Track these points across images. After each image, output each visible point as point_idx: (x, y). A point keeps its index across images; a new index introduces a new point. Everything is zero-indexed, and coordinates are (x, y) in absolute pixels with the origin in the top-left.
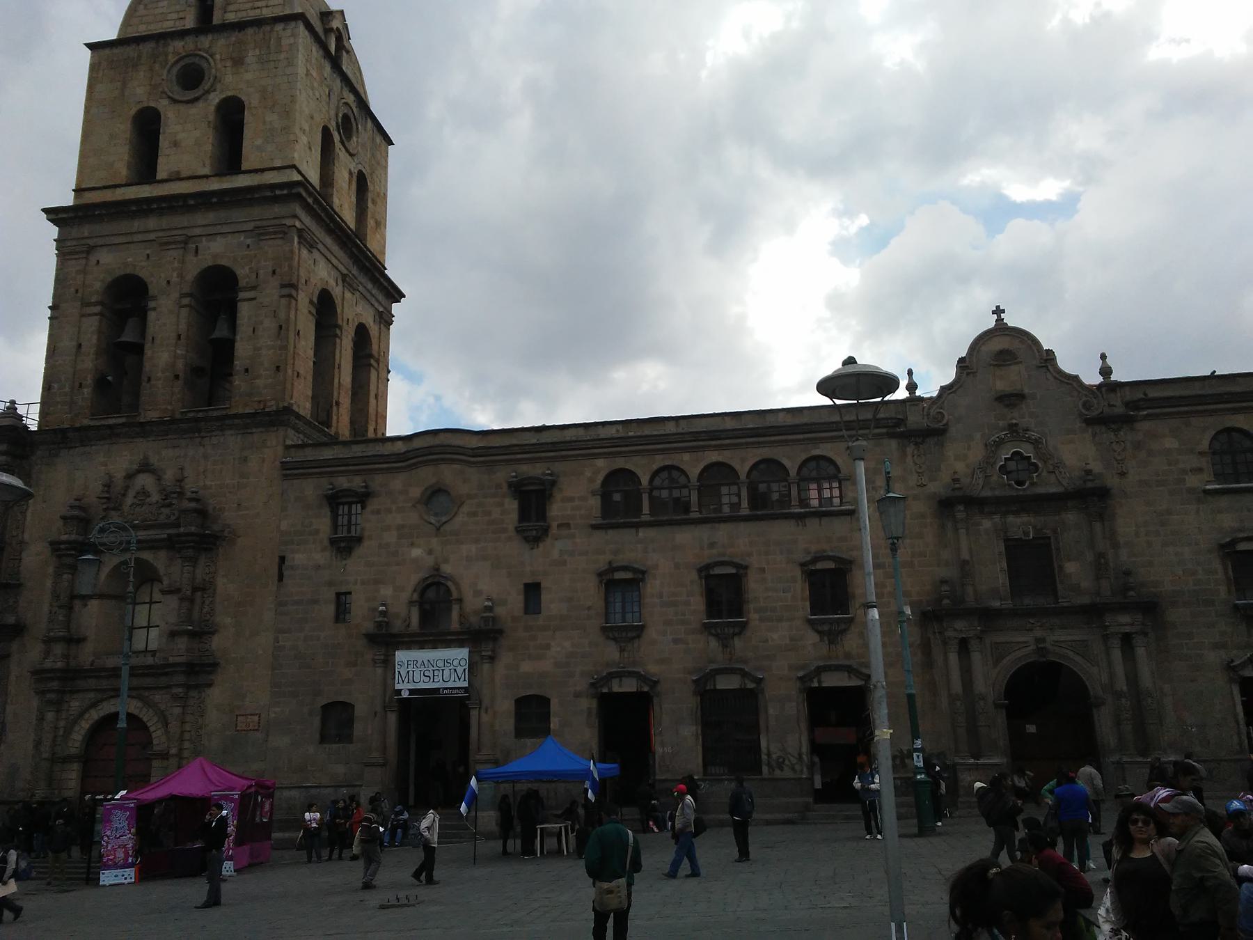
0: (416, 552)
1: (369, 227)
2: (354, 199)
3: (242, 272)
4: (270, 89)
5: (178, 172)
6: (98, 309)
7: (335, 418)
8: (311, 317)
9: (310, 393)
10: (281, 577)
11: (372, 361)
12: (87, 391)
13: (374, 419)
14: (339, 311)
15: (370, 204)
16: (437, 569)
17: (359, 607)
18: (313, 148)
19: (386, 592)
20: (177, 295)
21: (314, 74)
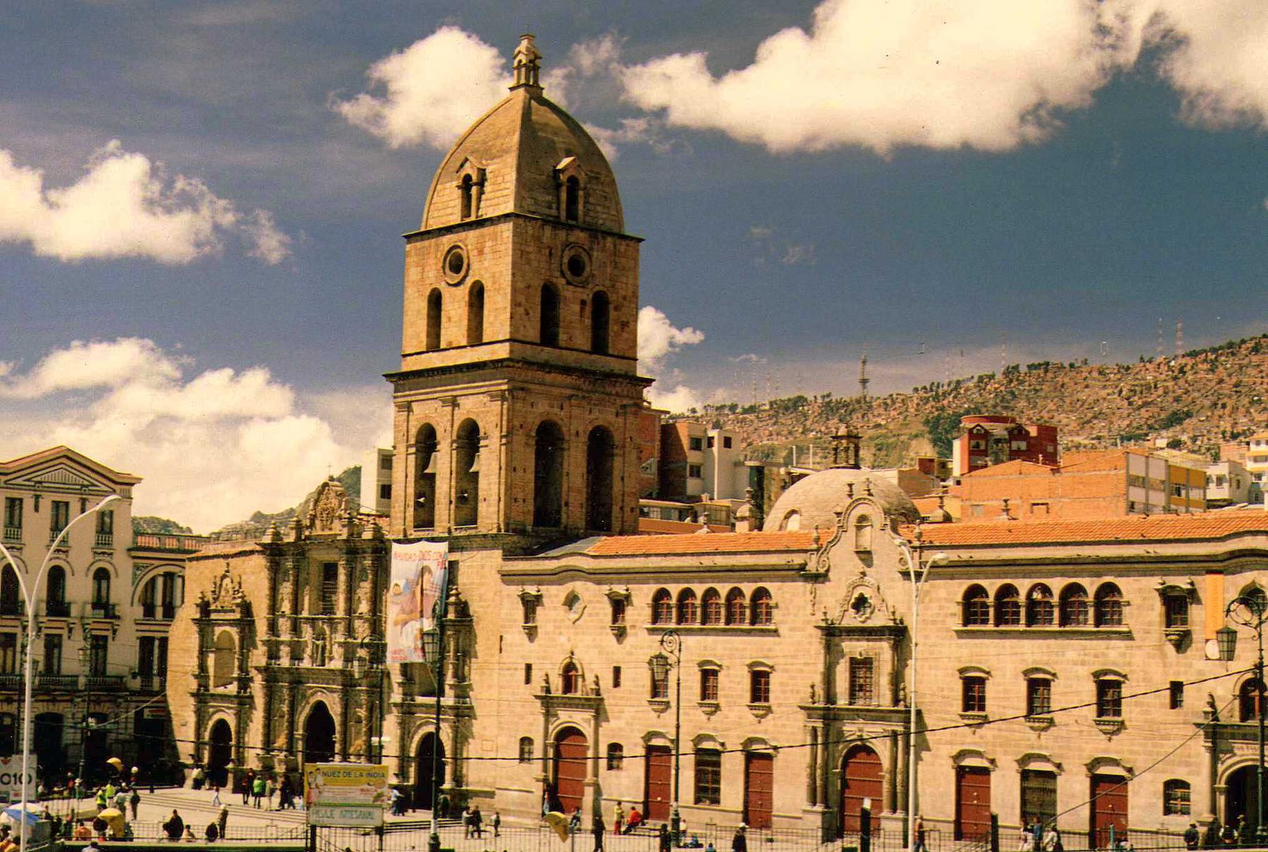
0: (563, 639)
1: (612, 334)
2: (588, 321)
3: (481, 425)
4: (497, 275)
5: (451, 343)
6: (413, 450)
7: (564, 516)
8: (528, 450)
9: (532, 508)
10: (501, 650)
11: (616, 451)
12: (411, 511)
13: (621, 498)
14: (564, 429)
15: (613, 314)
16: (572, 653)
17: (537, 676)
18: (531, 312)
19: (548, 667)
20: (449, 440)
21: (530, 249)
